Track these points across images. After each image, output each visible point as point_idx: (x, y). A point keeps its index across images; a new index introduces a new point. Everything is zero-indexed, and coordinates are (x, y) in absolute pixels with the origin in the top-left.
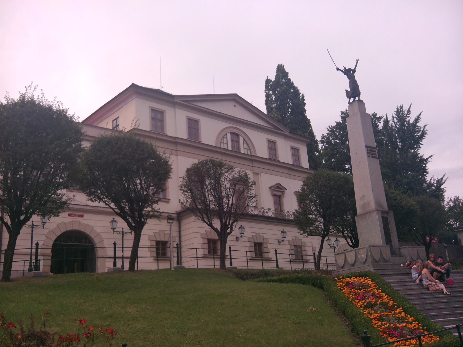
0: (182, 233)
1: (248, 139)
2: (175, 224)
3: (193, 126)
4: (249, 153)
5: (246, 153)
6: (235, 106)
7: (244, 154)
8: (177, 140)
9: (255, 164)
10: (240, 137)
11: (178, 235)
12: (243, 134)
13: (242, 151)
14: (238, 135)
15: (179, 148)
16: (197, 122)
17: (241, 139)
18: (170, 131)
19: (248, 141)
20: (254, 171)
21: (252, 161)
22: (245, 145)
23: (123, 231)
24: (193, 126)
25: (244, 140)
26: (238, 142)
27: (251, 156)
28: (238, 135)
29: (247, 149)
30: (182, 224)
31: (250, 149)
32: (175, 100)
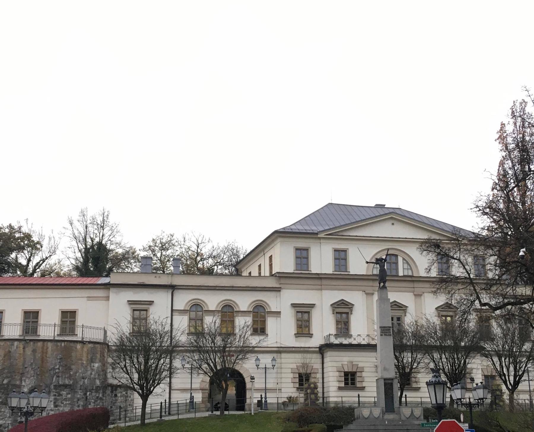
0: (325, 365)
1: (409, 259)
2: (319, 356)
3: (341, 257)
4: (410, 274)
5: (406, 274)
6: (393, 224)
7: (404, 276)
8: (320, 276)
9: (416, 285)
10: (399, 257)
11: (321, 367)
12: (402, 254)
13: (401, 274)
14: (396, 256)
15: (324, 282)
16: (345, 251)
17: (400, 260)
18: (315, 268)
19: (409, 262)
20: (415, 293)
21: (413, 281)
22: (406, 266)
23: (266, 368)
24: (341, 257)
25: (404, 259)
26: (396, 263)
27: (412, 276)
28: (396, 256)
29: (408, 269)
30: (325, 356)
31: (411, 269)
32: (319, 236)
